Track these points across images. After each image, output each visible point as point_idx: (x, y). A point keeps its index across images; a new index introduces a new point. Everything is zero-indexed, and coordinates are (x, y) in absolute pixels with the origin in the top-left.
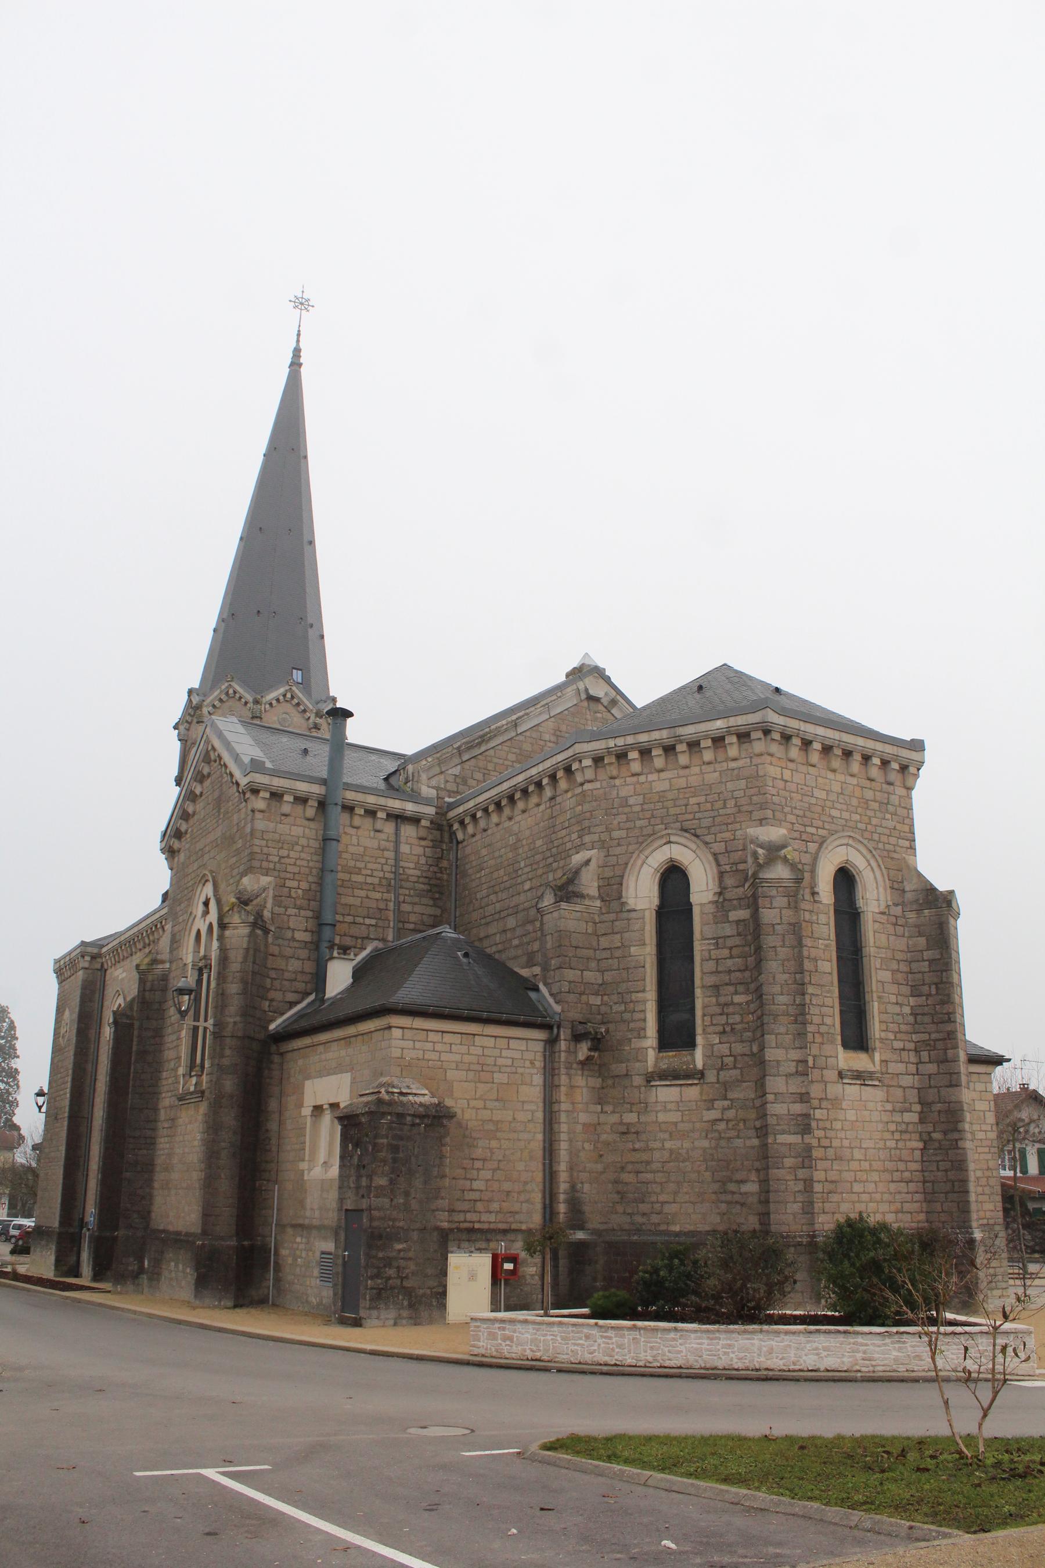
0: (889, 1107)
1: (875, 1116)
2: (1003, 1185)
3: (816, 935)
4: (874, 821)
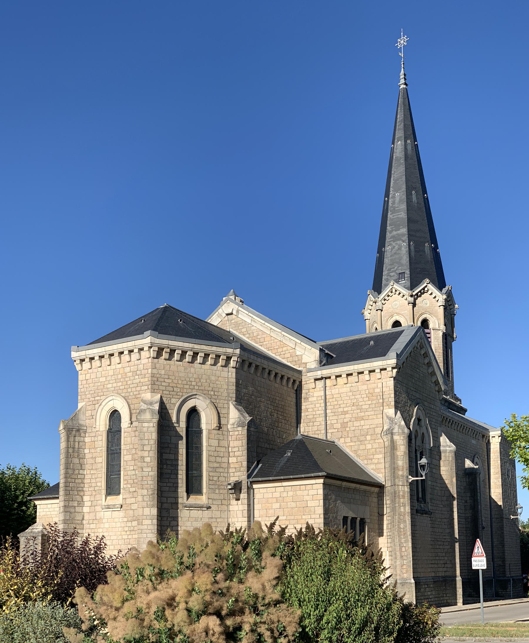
0: (125, 520)
1: (118, 525)
2: (522, 540)
3: (96, 447)
4: (129, 383)
